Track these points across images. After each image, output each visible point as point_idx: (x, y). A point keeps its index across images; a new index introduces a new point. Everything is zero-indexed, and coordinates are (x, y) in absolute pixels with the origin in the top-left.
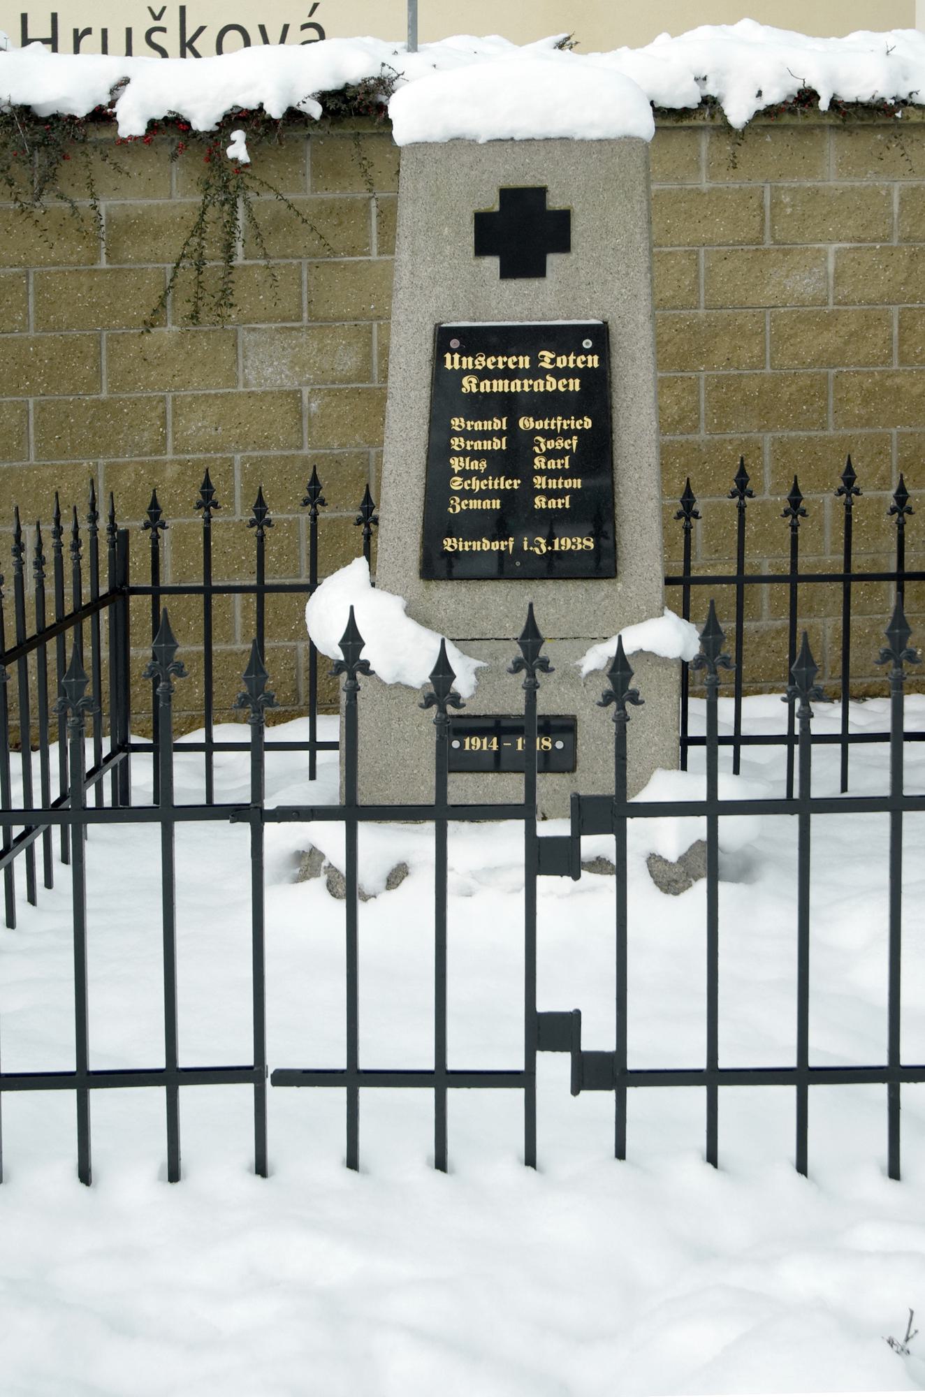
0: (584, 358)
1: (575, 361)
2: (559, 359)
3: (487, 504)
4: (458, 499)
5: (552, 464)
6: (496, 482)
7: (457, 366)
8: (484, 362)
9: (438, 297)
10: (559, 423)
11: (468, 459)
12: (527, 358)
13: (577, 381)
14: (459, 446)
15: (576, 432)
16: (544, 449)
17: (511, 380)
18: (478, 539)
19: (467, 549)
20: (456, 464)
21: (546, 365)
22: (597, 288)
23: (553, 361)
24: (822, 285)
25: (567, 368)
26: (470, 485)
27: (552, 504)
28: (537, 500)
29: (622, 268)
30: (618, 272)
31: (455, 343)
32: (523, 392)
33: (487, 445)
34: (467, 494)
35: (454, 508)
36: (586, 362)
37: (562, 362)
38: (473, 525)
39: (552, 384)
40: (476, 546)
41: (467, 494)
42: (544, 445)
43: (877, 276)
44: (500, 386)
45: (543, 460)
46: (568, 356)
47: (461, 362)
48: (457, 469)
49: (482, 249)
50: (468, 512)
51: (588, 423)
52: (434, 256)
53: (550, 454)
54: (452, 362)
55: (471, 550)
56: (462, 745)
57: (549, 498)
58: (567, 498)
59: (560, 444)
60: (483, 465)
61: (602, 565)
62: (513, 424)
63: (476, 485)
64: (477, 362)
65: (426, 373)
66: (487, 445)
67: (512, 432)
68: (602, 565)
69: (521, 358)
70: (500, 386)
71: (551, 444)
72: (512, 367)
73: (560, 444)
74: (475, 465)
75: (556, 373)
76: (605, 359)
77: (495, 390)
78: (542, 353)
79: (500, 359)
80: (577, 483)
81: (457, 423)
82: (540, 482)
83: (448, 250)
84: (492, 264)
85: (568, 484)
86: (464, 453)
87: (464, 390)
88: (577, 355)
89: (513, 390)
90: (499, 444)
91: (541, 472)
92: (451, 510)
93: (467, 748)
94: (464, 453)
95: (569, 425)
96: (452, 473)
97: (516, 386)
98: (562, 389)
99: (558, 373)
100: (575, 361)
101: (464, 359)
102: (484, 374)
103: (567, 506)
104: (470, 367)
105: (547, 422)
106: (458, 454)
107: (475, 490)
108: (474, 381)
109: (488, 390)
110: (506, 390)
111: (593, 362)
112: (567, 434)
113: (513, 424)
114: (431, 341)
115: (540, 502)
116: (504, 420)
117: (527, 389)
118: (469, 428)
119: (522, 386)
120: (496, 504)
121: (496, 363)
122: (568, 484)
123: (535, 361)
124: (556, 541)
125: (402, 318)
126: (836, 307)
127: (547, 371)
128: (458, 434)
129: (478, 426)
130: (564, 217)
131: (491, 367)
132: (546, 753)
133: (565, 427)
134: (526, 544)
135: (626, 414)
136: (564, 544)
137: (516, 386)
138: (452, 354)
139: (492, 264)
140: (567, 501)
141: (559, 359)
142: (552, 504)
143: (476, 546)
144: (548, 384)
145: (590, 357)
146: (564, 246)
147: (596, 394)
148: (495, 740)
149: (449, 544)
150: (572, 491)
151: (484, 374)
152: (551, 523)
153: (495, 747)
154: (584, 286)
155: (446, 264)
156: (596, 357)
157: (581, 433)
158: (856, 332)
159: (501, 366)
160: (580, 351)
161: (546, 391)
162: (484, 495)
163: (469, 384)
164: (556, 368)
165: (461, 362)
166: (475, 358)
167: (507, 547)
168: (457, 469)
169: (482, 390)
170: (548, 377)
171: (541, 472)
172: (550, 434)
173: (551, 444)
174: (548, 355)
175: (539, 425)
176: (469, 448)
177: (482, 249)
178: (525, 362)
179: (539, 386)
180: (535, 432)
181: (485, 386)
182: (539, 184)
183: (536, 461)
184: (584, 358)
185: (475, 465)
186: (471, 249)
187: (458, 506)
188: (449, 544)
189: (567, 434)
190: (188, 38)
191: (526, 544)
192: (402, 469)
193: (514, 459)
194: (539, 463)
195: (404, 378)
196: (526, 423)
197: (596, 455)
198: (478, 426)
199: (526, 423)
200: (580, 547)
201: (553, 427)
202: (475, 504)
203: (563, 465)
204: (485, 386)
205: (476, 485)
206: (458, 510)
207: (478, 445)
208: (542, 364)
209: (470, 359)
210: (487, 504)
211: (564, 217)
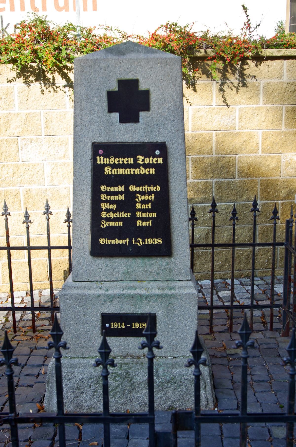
0: (156, 159)
1: (152, 161)
2: (145, 159)
4: (105, 222)
5: (144, 207)
6: (121, 214)
7: (102, 163)
8: (113, 160)
9: (93, 131)
10: (146, 188)
11: (108, 204)
12: (132, 159)
13: (154, 169)
14: (104, 198)
15: (153, 192)
16: (140, 200)
17: (125, 169)
18: (114, 239)
19: (109, 243)
20: (104, 206)
21: (140, 162)
22: (161, 127)
23: (143, 160)
24: (233, 122)
25: (149, 163)
26: (109, 215)
27: (144, 224)
28: (138, 222)
29: (172, 118)
30: (170, 120)
31: (101, 152)
32: (131, 174)
33: (116, 198)
34: (108, 219)
35: (103, 225)
36: (157, 161)
37: (147, 161)
38: (111, 233)
39: (143, 171)
40: (113, 242)
41: (108, 219)
42: (141, 198)
43: (254, 119)
44: (121, 171)
45: (140, 205)
46: (149, 158)
47: (104, 161)
48: (104, 208)
49: (111, 110)
50: (109, 227)
51: (158, 188)
52: (90, 111)
53: (143, 202)
55: (111, 244)
56: (110, 326)
57: (143, 221)
58: (151, 221)
59: (147, 198)
60: (115, 207)
61: (165, 250)
62: (127, 188)
63: (112, 215)
64: (111, 161)
65: (89, 166)
66: (116, 198)
67: (127, 192)
68: (165, 250)
69: (129, 159)
70: (121, 171)
71: (143, 198)
72: (126, 163)
73: (147, 198)
75: (145, 165)
77: (119, 173)
78: (138, 157)
79: (120, 159)
80: (155, 215)
81: (103, 188)
82: (139, 214)
83: (96, 109)
85: (151, 215)
86: (106, 201)
87: (105, 173)
88: (153, 158)
89: (126, 173)
90: (121, 197)
91: (139, 210)
92: (102, 226)
93: (112, 327)
94: (106, 201)
95: (150, 189)
96: (102, 210)
97: (128, 171)
98: (147, 173)
99: (146, 166)
100: (152, 161)
101: (105, 159)
102: (114, 166)
103: (151, 225)
104: (108, 163)
105: (141, 188)
106: (104, 202)
107: (112, 218)
108: (110, 169)
109: (116, 173)
110: (124, 173)
111: (160, 161)
112: (150, 193)
113: (127, 188)
114: (90, 150)
115: (139, 223)
116: (123, 187)
117: (132, 173)
118: (108, 190)
119: (130, 171)
120: (121, 224)
121: (119, 161)
122: (151, 215)
123: (135, 160)
124: (146, 240)
126: (239, 131)
127: (140, 165)
128: (104, 193)
129: (112, 189)
131: (117, 163)
133: (149, 190)
134: (134, 241)
135: (174, 184)
136: (150, 241)
137: (128, 171)
138: (100, 157)
139: (116, 116)
141: (145, 159)
142: (144, 224)
143: (113, 242)
144: (141, 171)
145: (159, 159)
147: (162, 175)
148: (123, 324)
149: (102, 241)
150: (152, 218)
151: (114, 166)
152: (145, 233)
153: (123, 327)
154: (155, 126)
155: (95, 115)
156: (161, 159)
157: (156, 193)
158: (246, 140)
159: (121, 162)
160: (154, 156)
161: (140, 174)
162: (115, 220)
163: (107, 171)
164: (144, 163)
165: (104, 161)
166: (110, 159)
167: (126, 242)
168: (104, 208)
169: (113, 173)
170: (141, 168)
171: (139, 210)
173: (143, 198)
174: (141, 158)
175: (138, 189)
176: (108, 199)
177: (111, 110)
178: (131, 161)
179: (137, 172)
180: (136, 192)
181: (115, 172)
182: (135, 78)
183: (137, 205)
184: (156, 159)
186: (106, 108)
187: (105, 225)
188: (102, 241)
189: (150, 193)
190: (4, 27)
191: (134, 241)
193: (128, 204)
194: (138, 206)
195: (80, 167)
196: (132, 188)
197: (162, 204)
198: (112, 189)
199: (132, 188)
200: (156, 243)
201: (144, 190)
202: (112, 224)
203: (148, 207)
204: (115, 172)
205: (112, 215)
206: (105, 226)
207: (112, 198)
208: (138, 162)
209: (108, 159)
211: (147, 93)
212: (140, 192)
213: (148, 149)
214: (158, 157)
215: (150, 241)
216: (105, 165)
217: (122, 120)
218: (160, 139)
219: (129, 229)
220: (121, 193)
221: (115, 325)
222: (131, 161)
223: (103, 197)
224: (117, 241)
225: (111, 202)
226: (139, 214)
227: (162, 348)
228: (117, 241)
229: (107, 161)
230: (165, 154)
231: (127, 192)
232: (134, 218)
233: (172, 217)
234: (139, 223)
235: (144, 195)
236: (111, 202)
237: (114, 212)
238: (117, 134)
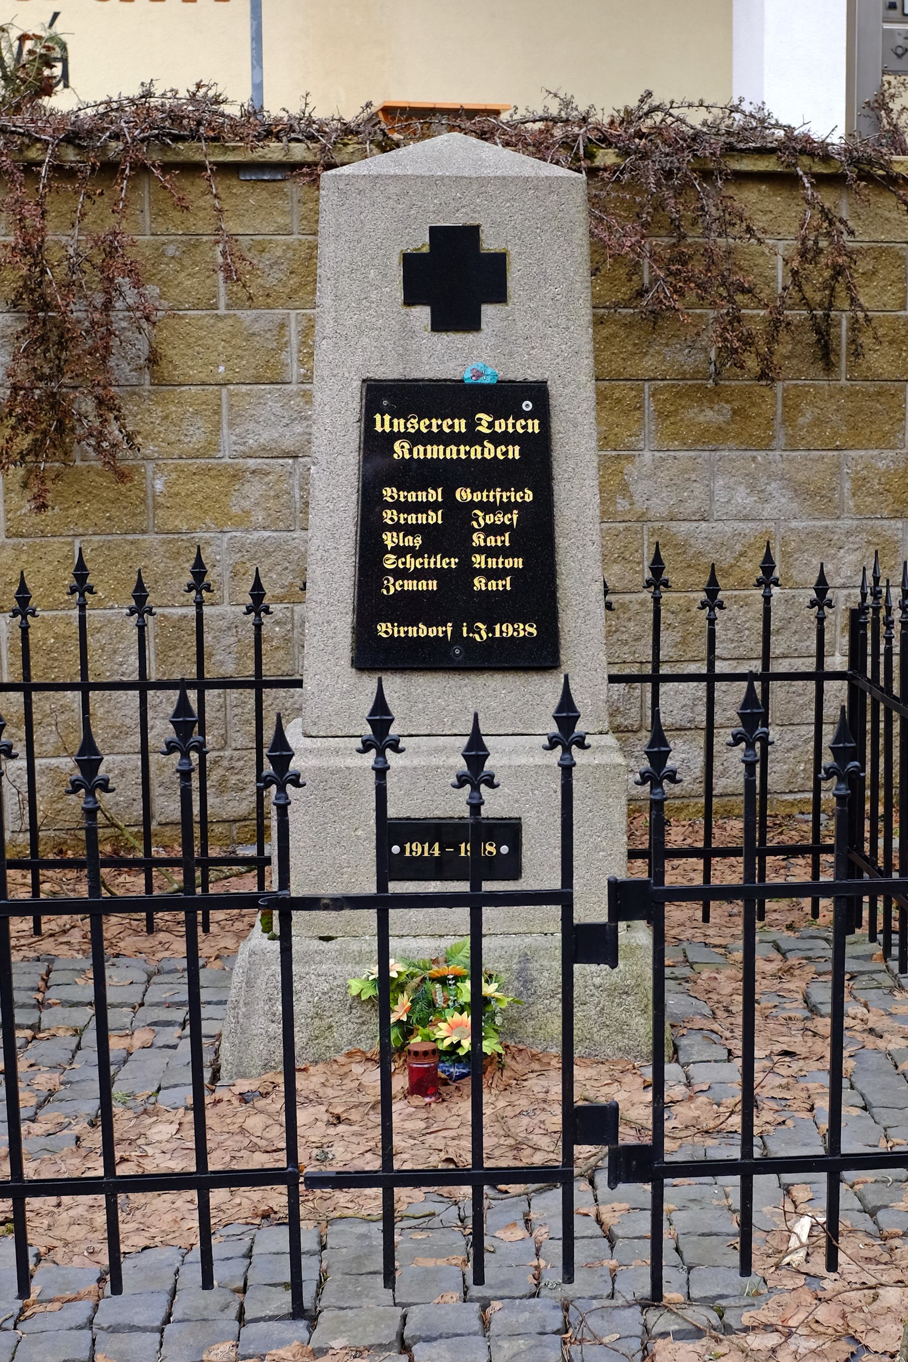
1: (514, 426)
3: (423, 585)
4: (392, 580)
5: (491, 541)
6: (432, 560)
9: (364, 349)
10: (498, 495)
11: (401, 535)
12: (463, 421)
15: (516, 505)
16: (482, 524)
17: (446, 446)
18: (414, 624)
19: (402, 635)
20: (390, 539)
21: (483, 429)
23: (491, 425)
26: (404, 563)
27: (492, 585)
29: (563, 322)
33: (422, 519)
34: (401, 574)
35: (388, 588)
37: (500, 426)
38: (409, 608)
39: (489, 451)
40: (412, 632)
41: (401, 574)
42: (483, 519)
44: (435, 452)
46: (506, 420)
47: (391, 425)
48: (390, 545)
49: (410, 300)
51: (529, 496)
53: (490, 530)
54: (383, 424)
55: (407, 636)
56: (403, 850)
57: (489, 579)
58: (508, 579)
59: (500, 519)
60: (418, 541)
62: (449, 494)
63: (411, 563)
64: (409, 425)
65: (353, 437)
66: (422, 519)
67: (449, 505)
70: (435, 452)
73: (500, 519)
74: (409, 541)
76: (545, 425)
77: (429, 456)
78: (479, 416)
80: (519, 563)
81: (389, 493)
82: (479, 560)
84: (422, 314)
85: (509, 563)
86: (397, 527)
87: (395, 456)
88: (516, 419)
90: (434, 518)
91: (480, 550)
93: (408, 854)
94: (397, 527)
95: (509, 497)
97: (452, 452)
99: (498, 439)
100: (514, 426)
101: (395, 421)
102: (416, 439)
106: (391, 528)
107: (412, 571)
108: (407, 446)
111: (534, 426)
112: (507, 508)
113: (449, 494)
115: (479, 583)
116: (440, 490)
118: (402, 500)
119: (458, 452)
120: (433, 585)
122: (509, 563)
123: (472, 424)
124: (497, 627)
125: (326, 373)
129: (412, 497)
130: (499, 261)
131: (425, 431)
132: (490, 859)
133: (505, 500)
134: (465, 629)
135: (568, 486)
136: (505, 630)
137: (452, 452)
138: (382, 415)
139: (422, 314)
140: (507, 583)
141: (497, 423)
142: (492, 585)
143: (412, 632)
144: (486, 450)
145: (530, 422)
146: (499, 295)
147: (535, 464)
148: (437, 845)
149: (384, 629)
151: (416, 439)
152: (493, 608)
153: (437, 853)
154: (521, 340)
156: (536, 422)
157: (521, 506)
160: (520, 415)
162: (419, 574)
163: (401, 449)
164: (494, 432)
165: (391, 425)
166: (407, 420)
167: (445, 632)
168: (390, 545)
171: (480, 550)
172: (488, 508)
174: (485, 418)
177: (410, 300)
178: (460, 425)
179: (476, 453)
180: (472, 505)
181: (419, 452)
183: (475, 536)
185: (409, 541)
186: (400, 295)
187: (392, 586)
188: (384, 629)
189: (507, 508)
191: (465, 629)
192: (330, 545)
193: (451, 536)
194: (478, 539)
196: (463, 495)
198: (412, 497)
199: (463, 495)
200: (522, 634)
202: (410, 585)
203: (503, 542)
204: (419, 452)
205: (411, 563)
206: (392, 591)
207: (412, 519)
208: (479, 428)
209: (402, 421)
210: (423, 585)
211: (499, 261)
212: (482, 506)
213: (505, 397)
214: (527, 416)
215: (505, 630)
216: (394, 436)
217: (439, 325)
218: (533, 375)
219: (453, 598)
220: (434, 506)
221: (416, 849)
222: (460, 425)
223: (389, 516)
224: (422, 631)
225: (410, 530)
226: (479, 560)
227: (589, 747)
228: (422, 631)
229: (399, 425)
230: (543, 412)
231: (449, 505)
232: (467, 571)
233: (561, 569)
234: (479, 583)
235: (494, 513)
236: (410, 530)
237: (416, 554)
238: (425, 358)
